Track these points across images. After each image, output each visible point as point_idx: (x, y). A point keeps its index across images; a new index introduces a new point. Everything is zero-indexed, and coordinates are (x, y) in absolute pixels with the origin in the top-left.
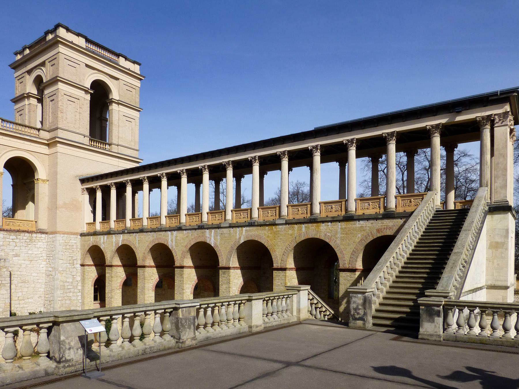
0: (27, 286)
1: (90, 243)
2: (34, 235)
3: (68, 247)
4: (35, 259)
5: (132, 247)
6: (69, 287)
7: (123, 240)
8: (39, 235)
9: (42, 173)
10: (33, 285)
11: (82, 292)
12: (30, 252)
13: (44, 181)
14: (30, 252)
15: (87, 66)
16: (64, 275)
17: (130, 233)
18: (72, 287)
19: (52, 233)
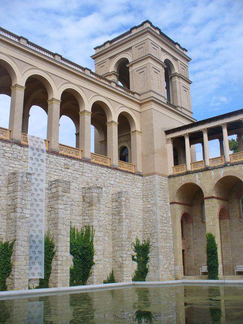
0: (133, 220)
1: (181, 183)
2: (136, 176)
4: (137, 197)
5: (238, 177)
7: (225, 173)
8: (138, 177)
9: (137, 126)
10: (136, 220)
11: (173, 226)
13: (138, 132)
14: (134, 191)
15: (162, 49)
16: (162, 210)
17: (233, 165)
18: (166, 222)
19: (148, 175)
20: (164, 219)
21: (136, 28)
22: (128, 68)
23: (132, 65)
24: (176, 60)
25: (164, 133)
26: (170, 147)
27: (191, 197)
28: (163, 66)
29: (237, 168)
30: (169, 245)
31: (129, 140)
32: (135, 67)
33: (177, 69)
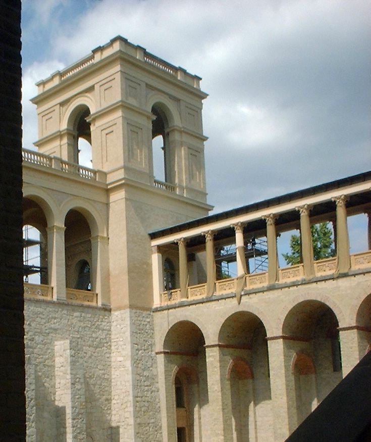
3: (141, 327)
6: (146, 384)
12: (94, 335)
14: (94, 335)
16: (140, 365)
17: (249, 294)
20: (143, 379)
21: (100, 49)
22: (89, 124)
23: (94, 120)
24: (177, 100)
25: (148, 237)
26: (156, 260)
27: (186, 344)
28: (148, 118)
29: (255, 298)
30: (153, 421)
31: (89, 249)
32: (98, 123)
33: (177, 120)
